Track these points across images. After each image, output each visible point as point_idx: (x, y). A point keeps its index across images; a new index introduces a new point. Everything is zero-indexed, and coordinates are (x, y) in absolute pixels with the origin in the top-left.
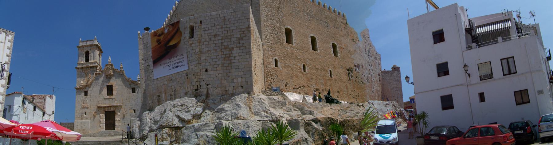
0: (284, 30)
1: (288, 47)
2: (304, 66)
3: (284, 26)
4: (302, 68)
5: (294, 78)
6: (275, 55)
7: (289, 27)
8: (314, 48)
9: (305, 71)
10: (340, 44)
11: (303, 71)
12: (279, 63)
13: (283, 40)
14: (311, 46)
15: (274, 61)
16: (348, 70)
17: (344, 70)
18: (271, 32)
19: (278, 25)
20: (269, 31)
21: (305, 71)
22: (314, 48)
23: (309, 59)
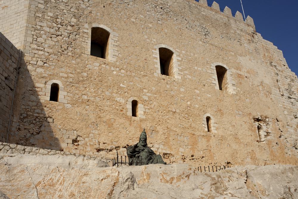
0: (90, 32)
1: (96, 63)
2: (135, 104)
3: (91, 23)
4: (130, 107)
5: (103, 127)
6: (52, 76)
7: (101, 26)
8: (165, 69)
9: (134, 114)
10: (237, 68)
11: (130, 113)
12: (61, 95)
13: (82, 48)
14: (158, 66)
15: (49, 87)
16: (258, 120)
17: (246, 119)
18: (52, 31)
19: (74, 20)
20: (48, 29)
21: (134, 114)
22: (165, 69)
23: (150, 91)
